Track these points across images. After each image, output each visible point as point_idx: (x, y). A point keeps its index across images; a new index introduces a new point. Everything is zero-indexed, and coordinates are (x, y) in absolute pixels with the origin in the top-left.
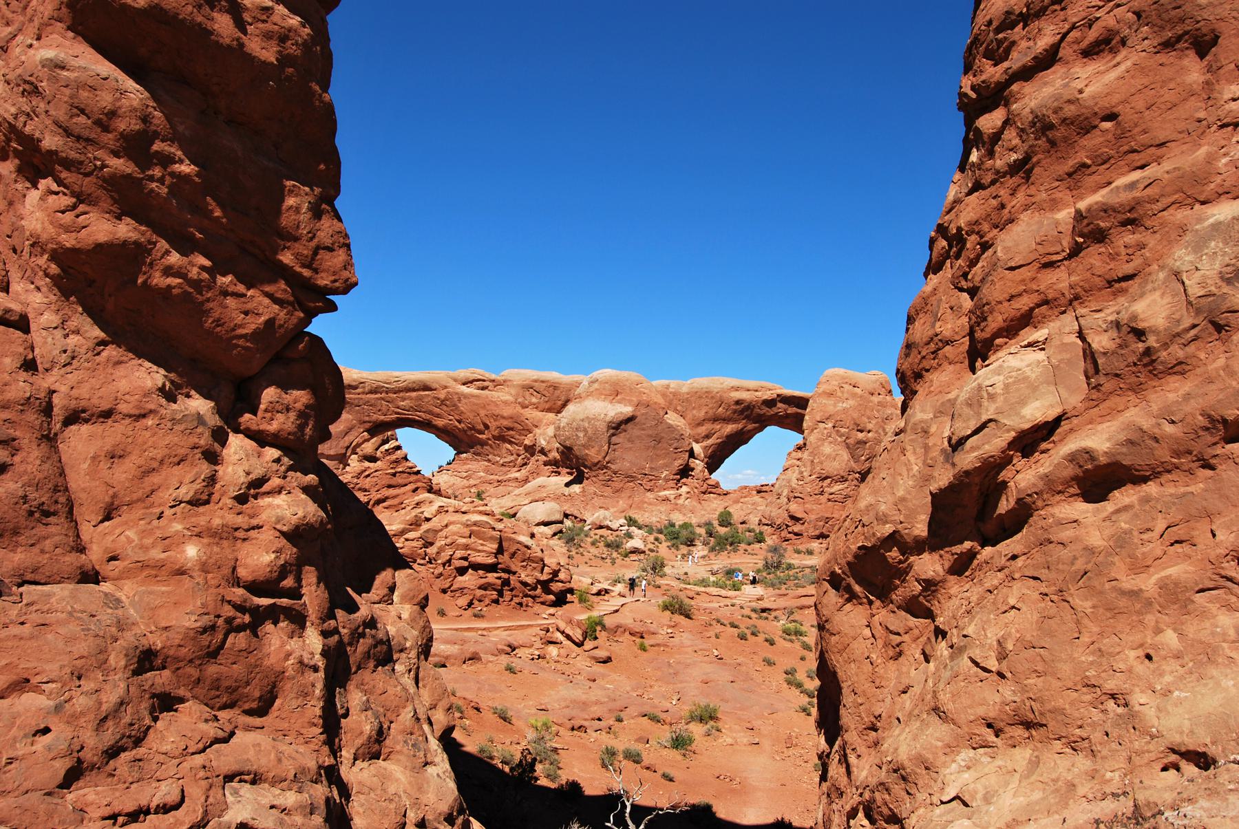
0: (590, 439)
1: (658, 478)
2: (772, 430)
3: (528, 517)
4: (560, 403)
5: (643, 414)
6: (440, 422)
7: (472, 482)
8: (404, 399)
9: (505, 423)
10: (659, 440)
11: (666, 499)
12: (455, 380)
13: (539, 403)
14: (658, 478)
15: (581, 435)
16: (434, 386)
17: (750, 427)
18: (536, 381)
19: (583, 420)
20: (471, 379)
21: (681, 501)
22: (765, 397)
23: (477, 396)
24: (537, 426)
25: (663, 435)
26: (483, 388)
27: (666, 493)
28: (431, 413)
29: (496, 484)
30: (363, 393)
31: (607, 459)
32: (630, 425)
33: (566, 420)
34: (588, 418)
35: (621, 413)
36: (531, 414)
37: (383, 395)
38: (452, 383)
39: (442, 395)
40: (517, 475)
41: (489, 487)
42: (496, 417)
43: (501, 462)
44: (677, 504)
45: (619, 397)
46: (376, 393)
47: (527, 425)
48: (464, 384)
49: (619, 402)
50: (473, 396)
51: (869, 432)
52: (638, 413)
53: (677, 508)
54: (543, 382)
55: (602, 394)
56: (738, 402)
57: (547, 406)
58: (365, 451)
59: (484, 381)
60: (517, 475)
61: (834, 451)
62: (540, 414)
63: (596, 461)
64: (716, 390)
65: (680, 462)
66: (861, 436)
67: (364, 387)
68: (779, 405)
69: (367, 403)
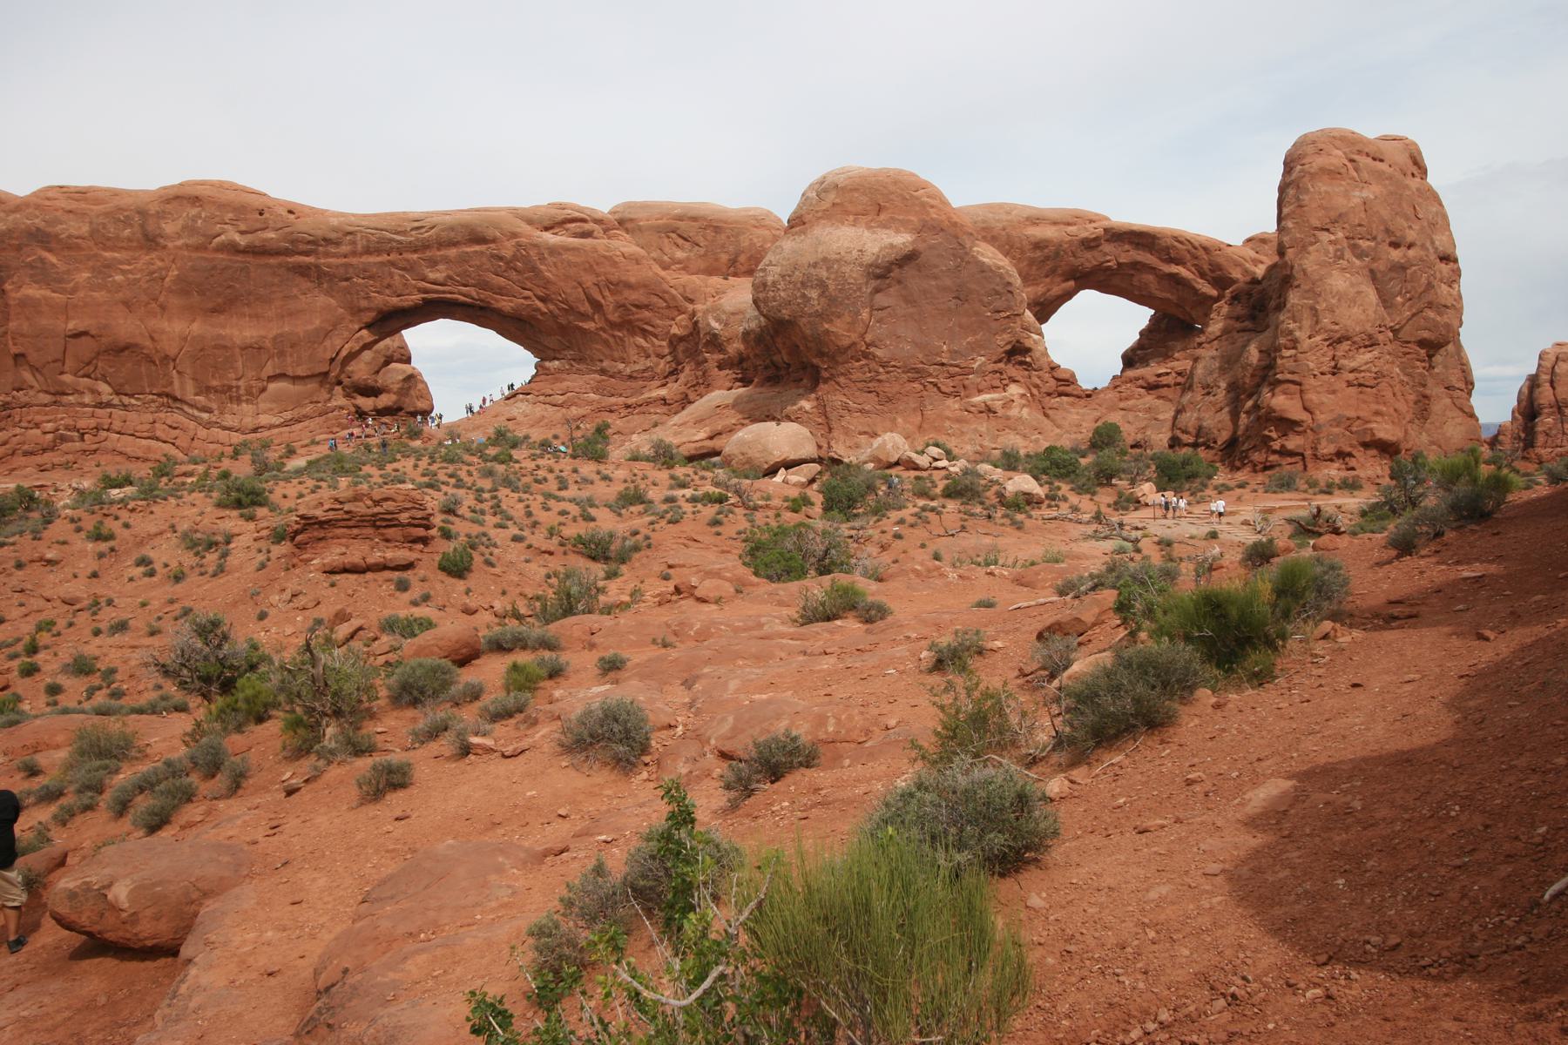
0: (832, 301)
1: (967, 371)
2: (1088, 300)
3: (751, 453)
4: (724, 258)
5: (932, 247)
6: (506, 304)
7: (575, 411)
8: (433, 263)
9: (634, 296)
10: (961, 296)
11: (989, 410)
12: (530, 222)
13: (688, 259)
14: (967, 371)
15: (814, 294)
16: (491, 233)
17: (1056, 290)
18: (680, 218)
19: (815, 265)
20: (560, 218)
21: (1014, 412)
22: (1084, 234)
23: (574, 249)
24: (691, 301)
25: (973, 286)
26: (587, 234)
27: (986, 397)
28: (484, 285)
29: (624, 412)
30: (354, 253)
31: (868, 338)
32: (909, 271)
33: (778, 269)
34: (825, 260)
35: (892, 246)
36: (676, 280)
37: (394, 257)
38: (525, 228)
39: (507, 250)
40: (663, 392)
41: (610, 419)
42: (616, 286)
43: (628, 371)
44: (1008, 418)
45: (883, 217)
46: (378, 252)
47: (674, 297)
48: (546, 229)
49: (885, 226)
50: (567, 249)
51: (1410, 246)
52: (921, 246)
53: (1010, 425)
54: (694, 219)
55: (847, 213)
56: (1038, 245)
57: (702, 264)
58: (355, 377)
59: (583, 220)
60: (663, 392)
61: (1352, 285)
62: (697, 280)
63: (846, 342)
64: (1000, 225)
65: (1006, 337)
66: (1396, 255)
67: (354, 243)
68: (1107, 247)
69: (365, 272)
